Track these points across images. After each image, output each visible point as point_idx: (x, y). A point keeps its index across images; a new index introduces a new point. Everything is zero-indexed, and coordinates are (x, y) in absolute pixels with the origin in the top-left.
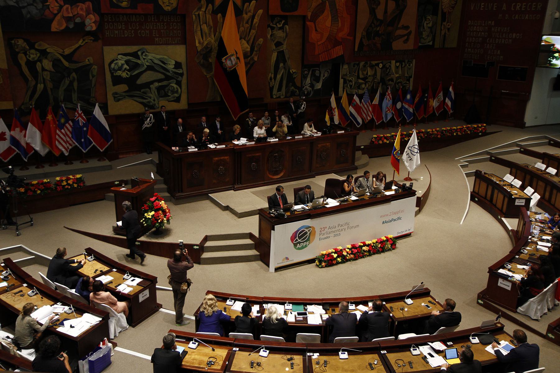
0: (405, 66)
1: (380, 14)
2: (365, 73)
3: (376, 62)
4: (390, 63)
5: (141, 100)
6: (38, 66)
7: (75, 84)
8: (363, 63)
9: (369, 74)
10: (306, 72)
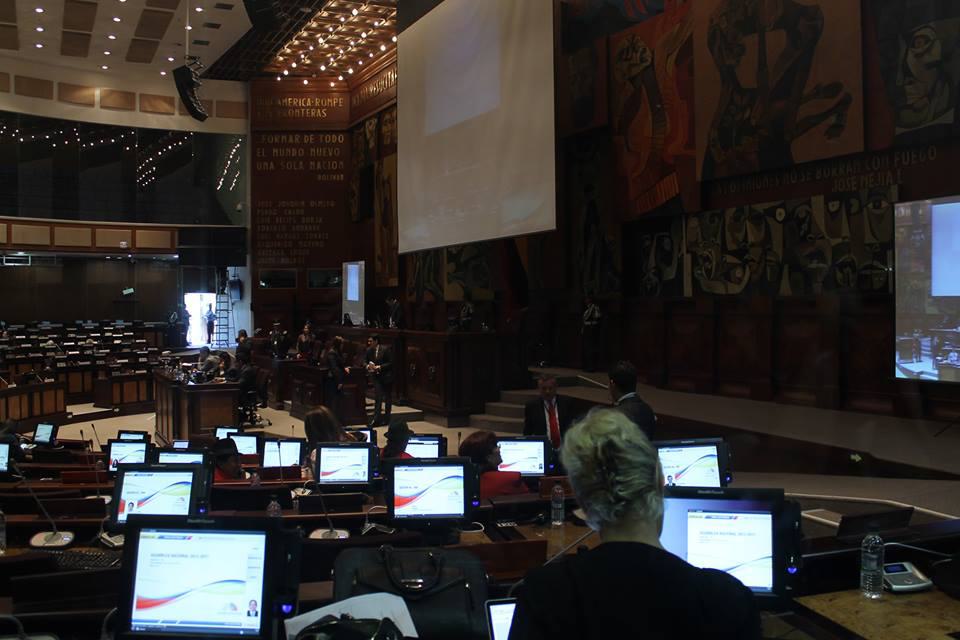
0: (861, 210)
1: (747, 76)
2: (740, 236)
3: (767, 205)
4: (809, 203)
8: (734, 209)
9: (751, 239)
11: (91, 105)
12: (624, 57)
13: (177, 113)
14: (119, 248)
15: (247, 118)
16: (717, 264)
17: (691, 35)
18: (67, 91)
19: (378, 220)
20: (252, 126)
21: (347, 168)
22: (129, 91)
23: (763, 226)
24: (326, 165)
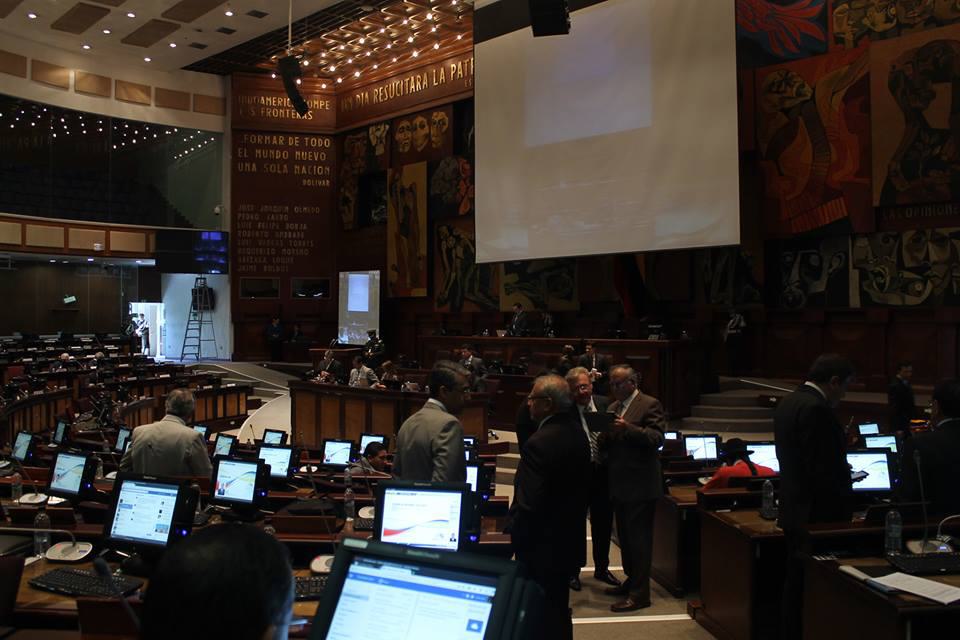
2: (921, 256)
5: (530, 294)
6: (454, 251)
7: (478, 273)
8: (911, 233)
9: (933, 257)
10: (789, 259)
11: (65, 88)
12: (774, 89)
13: (153, 104)
14: (93, 251)
15: (224, 114)
16: (892, 278)
17: (868, 75)
18: (41, 70)
19: (392, 228)
20: (233, 123)
21: (401, 180)
22: (106, 75)
23: (949, 248)
24: (312, 169)
